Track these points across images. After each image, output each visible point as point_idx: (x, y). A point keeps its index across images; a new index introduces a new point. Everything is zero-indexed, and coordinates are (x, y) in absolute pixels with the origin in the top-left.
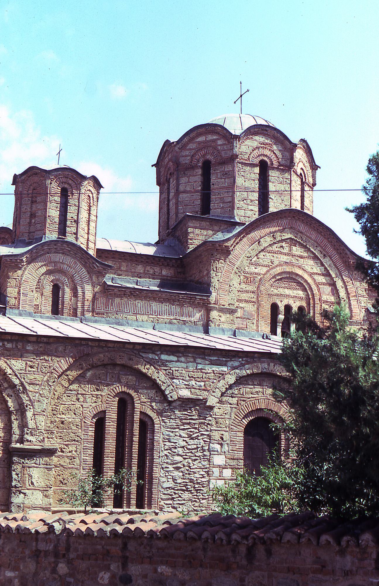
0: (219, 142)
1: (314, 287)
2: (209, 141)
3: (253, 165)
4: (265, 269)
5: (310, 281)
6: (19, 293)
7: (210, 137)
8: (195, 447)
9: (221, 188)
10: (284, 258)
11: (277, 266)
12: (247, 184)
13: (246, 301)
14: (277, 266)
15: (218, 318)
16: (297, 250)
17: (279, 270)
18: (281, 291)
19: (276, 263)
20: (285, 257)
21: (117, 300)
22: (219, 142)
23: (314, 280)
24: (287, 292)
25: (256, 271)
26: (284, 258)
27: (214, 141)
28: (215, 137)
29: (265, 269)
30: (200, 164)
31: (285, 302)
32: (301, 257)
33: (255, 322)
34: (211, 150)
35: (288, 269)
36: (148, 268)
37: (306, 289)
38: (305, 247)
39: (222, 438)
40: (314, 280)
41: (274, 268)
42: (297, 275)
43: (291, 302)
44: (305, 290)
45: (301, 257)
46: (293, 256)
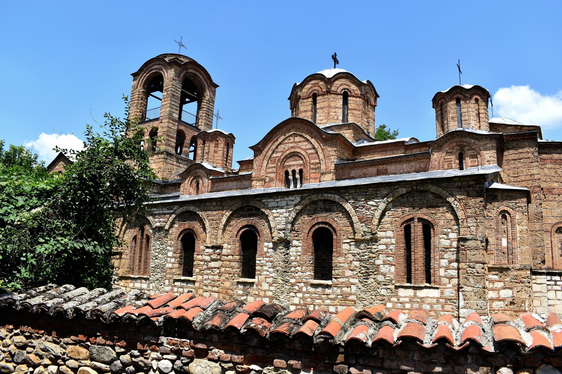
3: (308, 98)
4: (281, 154)
5: (304, 153)
10: (291, 145)
16: (297, 139)
18: (290, 163)
19: (286, 149)
20: (291, 144)
21: (216, 184)
23: (307, 153)
25: (276, 155)
26: (291, 145)
31: (292, 168)
32: (300, 142)
33: (274, 182)
35: (292, 150)
38: (301, 136)
40: (307, 153)
42: (298, 152)
43: (295, 168)
44: (302, 160)
45: (300, 142)
46: (295, 142)
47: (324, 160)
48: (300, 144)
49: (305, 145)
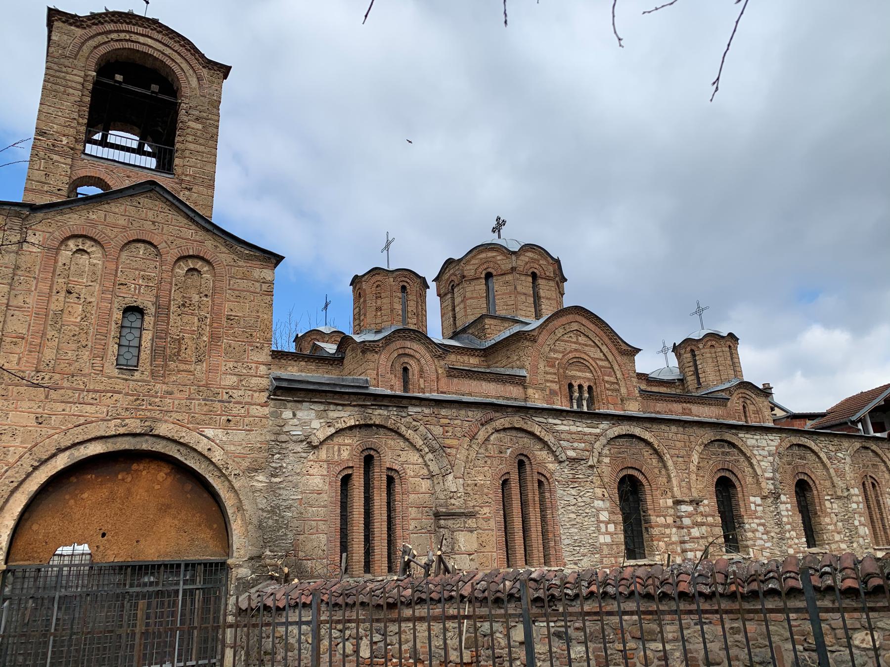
0: (499, 258)
1: (597, 369)
2: (489, 258)
6: (377, 374)
7: (490, 254)
8: (583, 504)
9: (504, 294)
11: (569, 353)
12: (524, 291)
13: (552, 382)
14: (569, 353)
15: (532, 395)
17: (571, 355)
22: (499, 258)
24: (579, 374)
27: (493, 257)
28: (495, 254)
29: (560, 356)
30: (483, 276)
34: (492, 265)
36: (459, 357)
37: (591, 371)
39: (604, 495)
41: (568, 354)
47: (623, 380)
48: (586, 349)
49: (595, 353)
